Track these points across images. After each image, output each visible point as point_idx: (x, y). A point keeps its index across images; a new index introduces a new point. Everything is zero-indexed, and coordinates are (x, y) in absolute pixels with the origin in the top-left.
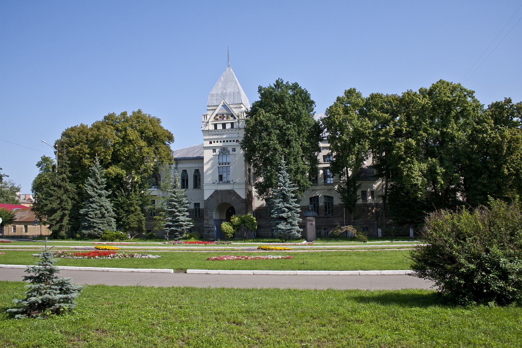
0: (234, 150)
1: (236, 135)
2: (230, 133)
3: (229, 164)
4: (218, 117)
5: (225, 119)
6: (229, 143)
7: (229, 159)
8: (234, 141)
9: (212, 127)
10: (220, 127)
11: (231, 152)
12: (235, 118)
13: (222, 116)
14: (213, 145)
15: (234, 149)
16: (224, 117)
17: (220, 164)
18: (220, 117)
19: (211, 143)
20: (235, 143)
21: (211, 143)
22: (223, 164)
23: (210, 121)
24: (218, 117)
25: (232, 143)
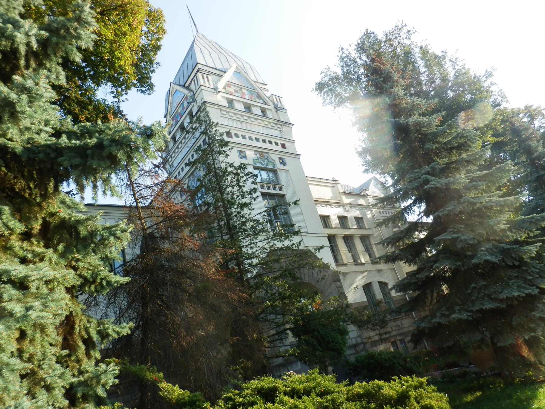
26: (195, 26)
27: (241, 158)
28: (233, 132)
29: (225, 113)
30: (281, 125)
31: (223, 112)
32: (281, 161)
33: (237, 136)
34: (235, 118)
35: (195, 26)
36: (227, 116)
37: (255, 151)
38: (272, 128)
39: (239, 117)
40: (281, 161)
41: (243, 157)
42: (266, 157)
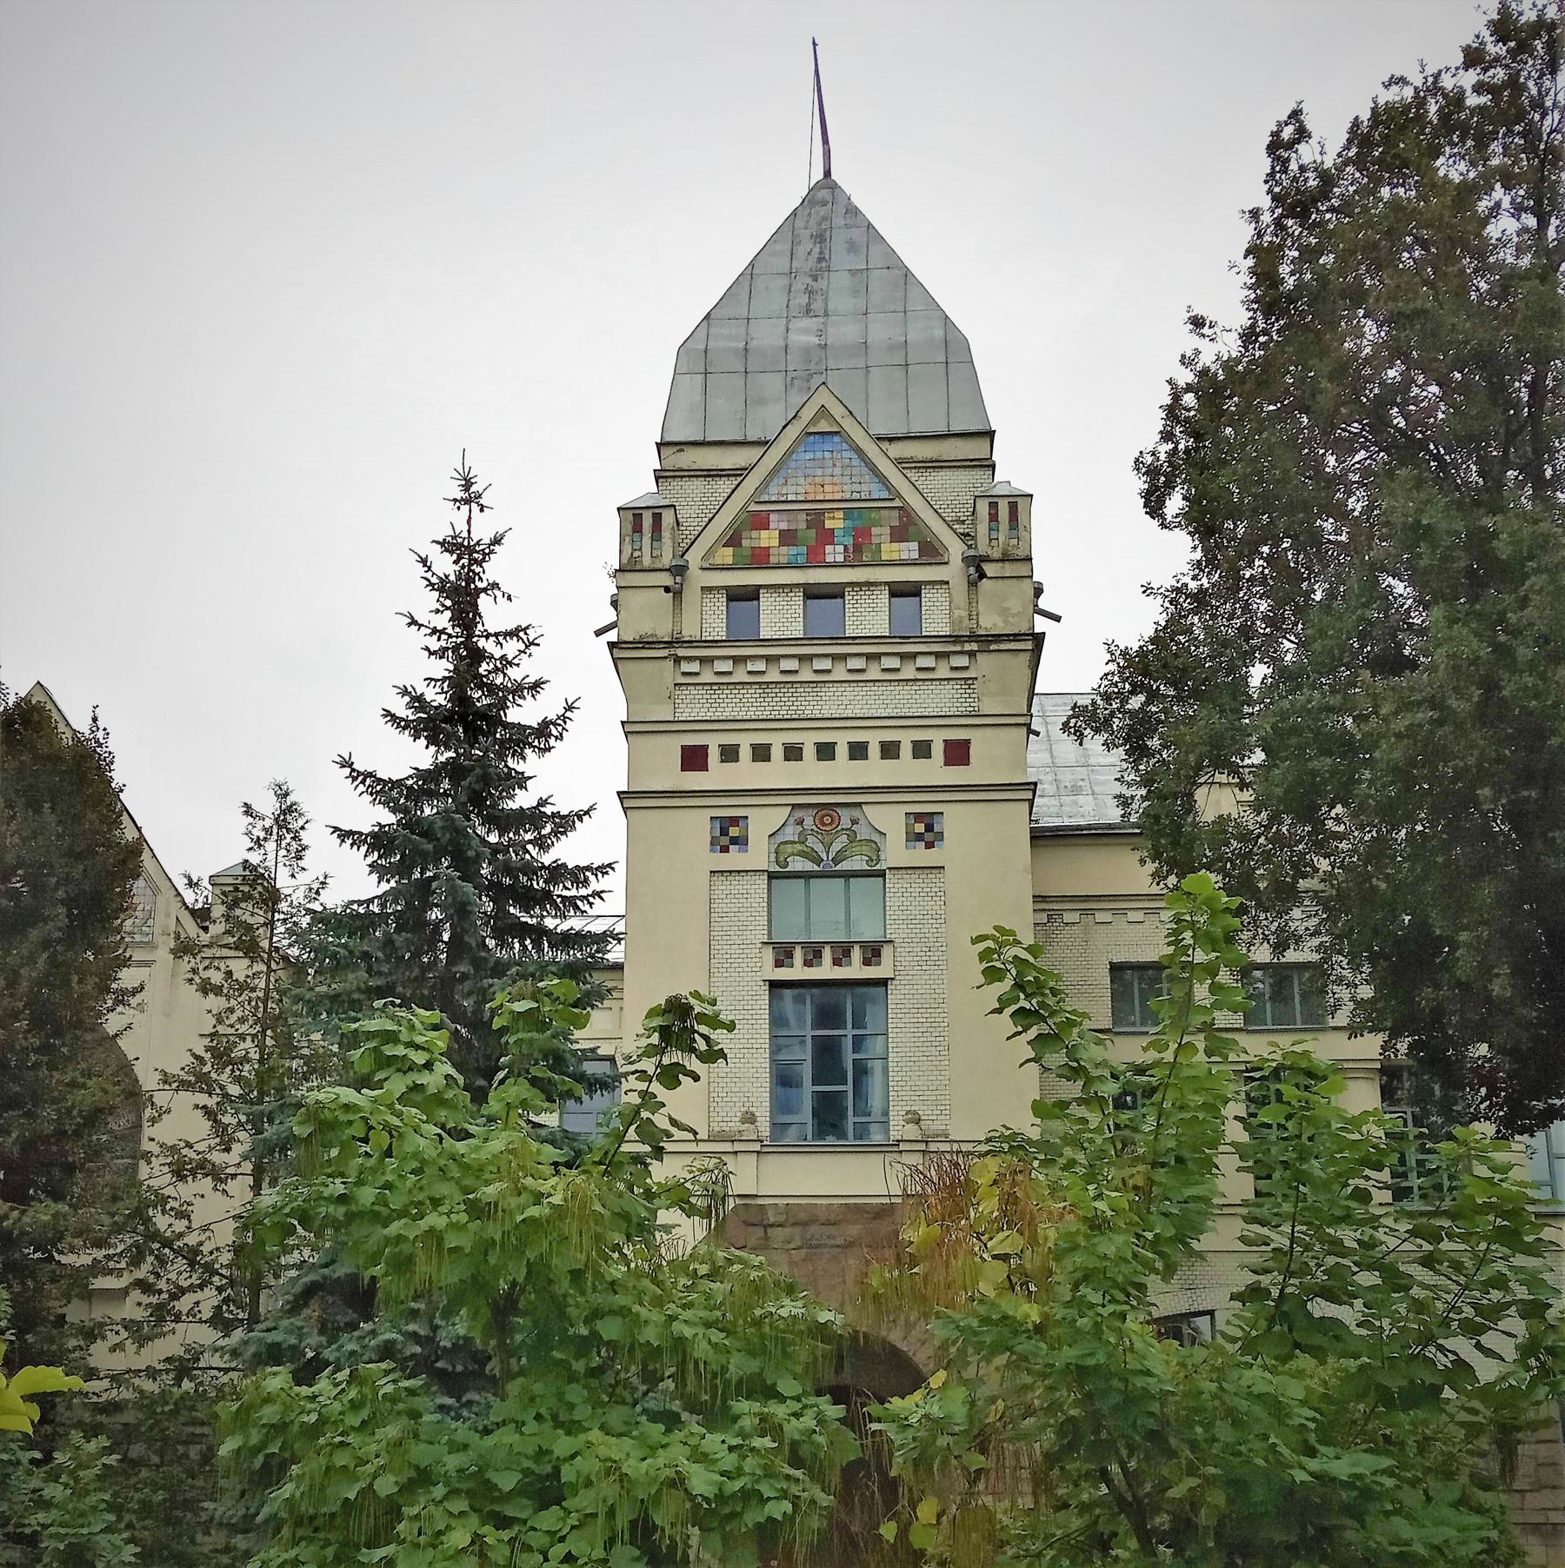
0: (926, 831)
1: (940, 699)
2: (892, 678)
3: (873, 953)
4: (768, 539)
5: (834, 553)
6: (876, 771)
7: (899, 912)
8: (922, 750)
9: (712, 620)
10: (780, 617)
11: (896, 851)
12: (931, 552)
13: (811, 537)
14: (717, 775)
15: (929, 820)
16: (828, 537)
17: (783, 955)
18: (787, 538)
19: (694, 759)
20: (934, 771)
21: (694, 759)
22: (814, 954)
23: (694, 558)
24: (768, 539)
25: (907, 771)
26: (825, 141)
27: (725, 849)
28: (713, 743)
29: (694, 667)
30: (972, 654)
31: (686, 667)
32: (920, 828)
33: (730, 754)
34: (740, 676)
35: (825, 141)
36: (707, 677)
37: (794, 806)
38: (925, 677)
39: (761, 666)
40: (920, 828)
41: (734, 841)
42: (845, 823)
